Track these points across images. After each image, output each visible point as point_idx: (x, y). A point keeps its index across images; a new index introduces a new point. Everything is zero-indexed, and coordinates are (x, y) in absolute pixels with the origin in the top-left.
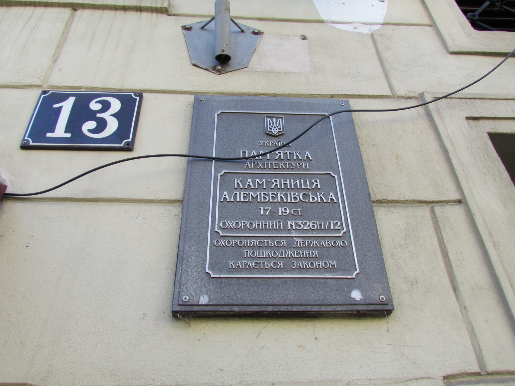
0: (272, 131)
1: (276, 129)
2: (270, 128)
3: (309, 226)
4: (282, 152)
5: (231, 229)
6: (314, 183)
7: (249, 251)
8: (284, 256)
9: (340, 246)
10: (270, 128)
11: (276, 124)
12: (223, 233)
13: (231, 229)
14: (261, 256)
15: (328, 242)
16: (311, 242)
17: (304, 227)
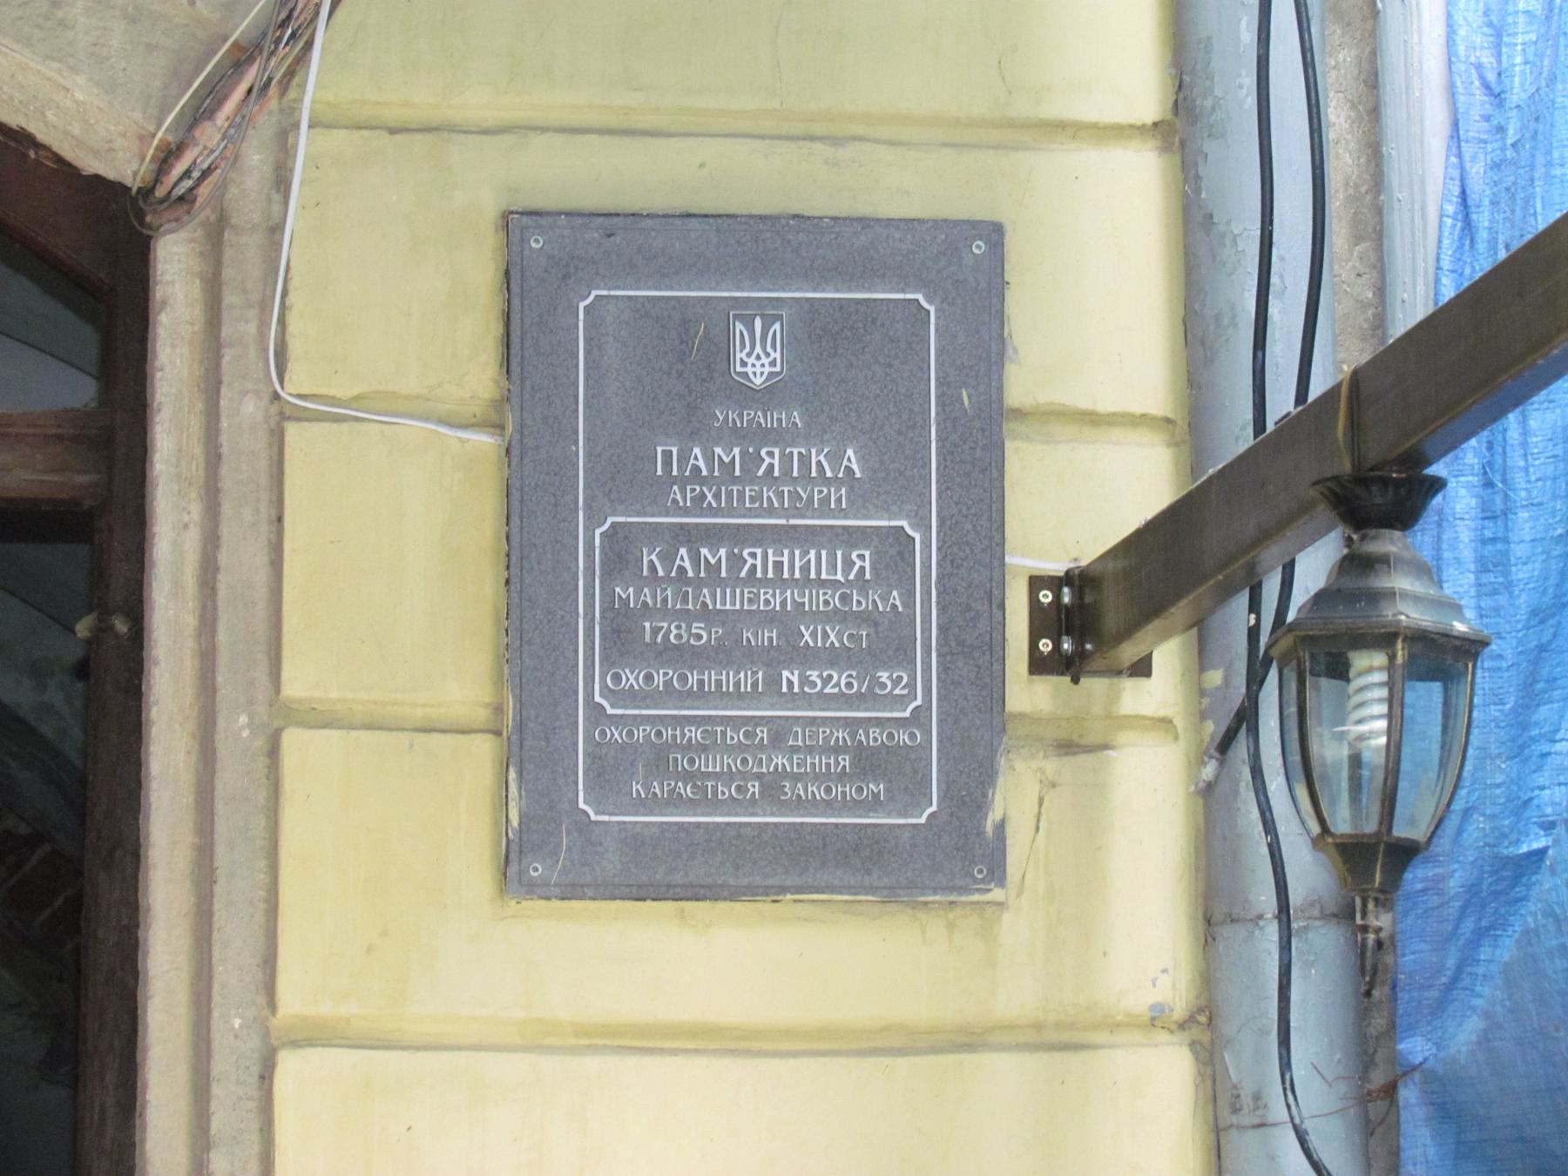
0: (747, 373)
1: (763, 365)
2: (741, 359)
3: (838, 684)
4: (777, 451)
5: (631, 697)
6: (855, 563)
7: (679, 757)
8: (764, 770)
9: (901, 743)
10: (744, 364)
11: (764, 348)
12: (612, 706)
13: (631, 697)
14: (710, 769)
15: (874, 732)
16: (831, 731)
17: (824, 687)
